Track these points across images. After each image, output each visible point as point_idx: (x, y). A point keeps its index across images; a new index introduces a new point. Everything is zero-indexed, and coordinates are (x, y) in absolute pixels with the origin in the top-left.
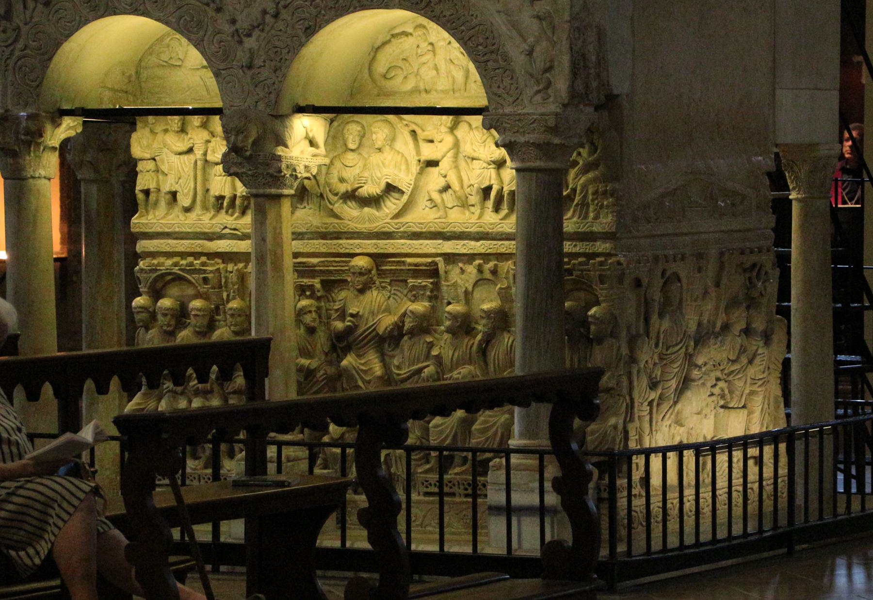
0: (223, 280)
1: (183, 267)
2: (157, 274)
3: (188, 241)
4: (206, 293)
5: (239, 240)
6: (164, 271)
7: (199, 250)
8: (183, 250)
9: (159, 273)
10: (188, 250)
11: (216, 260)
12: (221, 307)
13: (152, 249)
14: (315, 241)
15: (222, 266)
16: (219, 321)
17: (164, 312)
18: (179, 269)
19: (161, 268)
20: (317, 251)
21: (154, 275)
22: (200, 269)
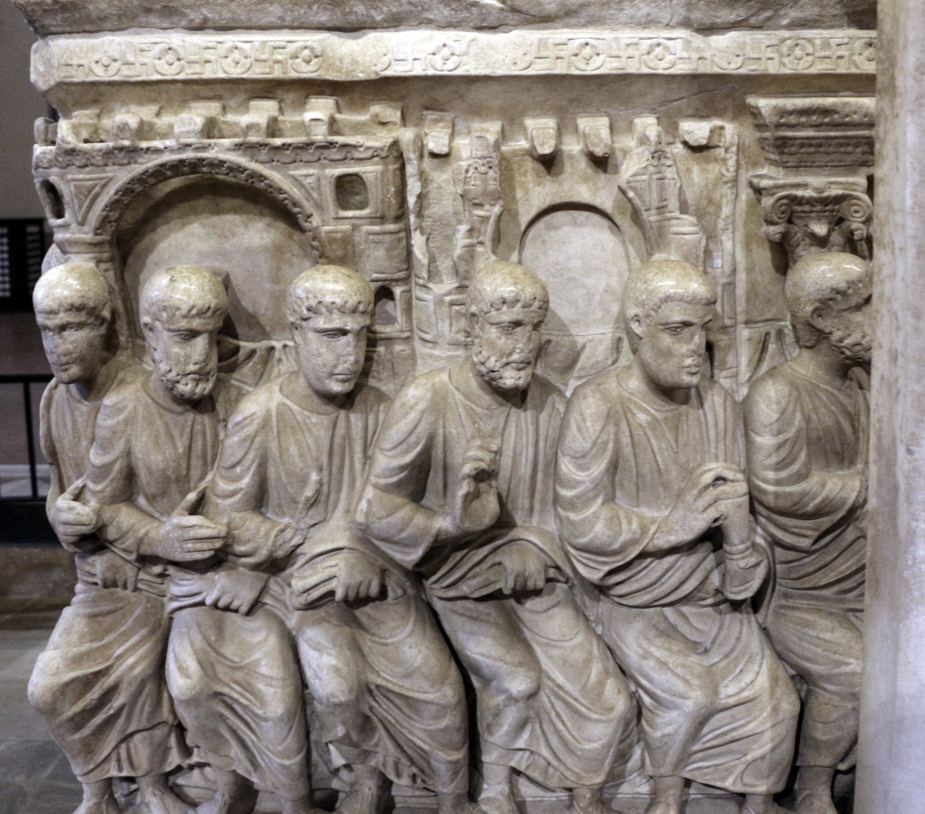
0: (414, 187)
1: (253, 138)
2: (137, 169)
3: (258, 37)
4: (347, 241)
5: (479, 29)
6: (167, 158)
7: (308, 71)
8: (236, 72)
9: (150, 163)
10: (258, 72)
11: (376, 109)
12: (398, 291)
13: (101, 75)
14: (826, 33)
15: (406, 135)
16: (389, 340)
17: (184, 324)
18: (238, 147)
19: (158, 144)
20: (842, 70)
21: (122, 176)
22: (330, 145)
